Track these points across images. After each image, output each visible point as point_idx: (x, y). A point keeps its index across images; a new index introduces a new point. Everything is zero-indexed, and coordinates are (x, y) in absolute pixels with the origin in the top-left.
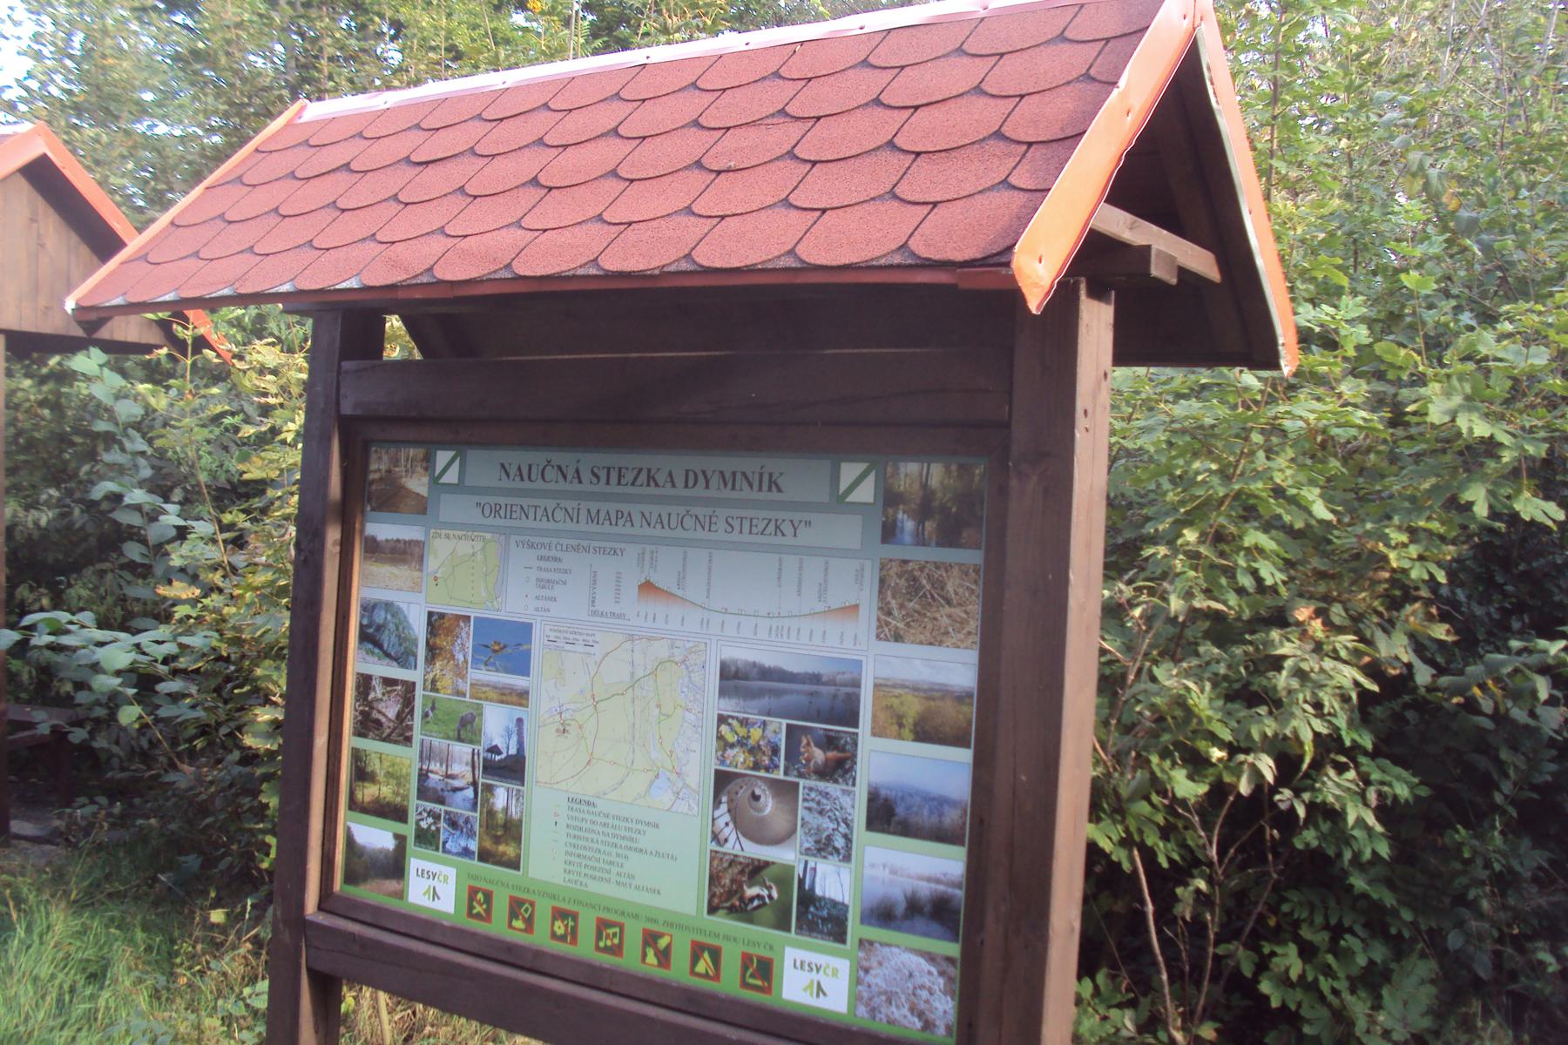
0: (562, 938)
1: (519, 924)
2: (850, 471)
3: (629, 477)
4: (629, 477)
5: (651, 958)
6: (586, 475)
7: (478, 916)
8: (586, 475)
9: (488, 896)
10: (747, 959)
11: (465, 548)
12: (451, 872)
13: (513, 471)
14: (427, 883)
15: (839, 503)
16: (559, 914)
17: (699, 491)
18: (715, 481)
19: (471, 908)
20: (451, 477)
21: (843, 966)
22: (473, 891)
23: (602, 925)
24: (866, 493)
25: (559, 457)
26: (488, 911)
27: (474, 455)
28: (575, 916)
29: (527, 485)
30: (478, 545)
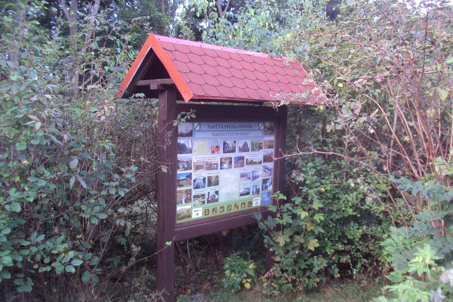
0: (222, 212)
1: (214, 213)
2: (261, 124)
3: (231, 127)
4: (231, 127)
5: (236, 208)
6: (224, 127)
7: (207, 215)
8: (224, 127)
9: (208, 210)
10: (249, 202)
11: (201, 143)
12: (201, 209)
13: (210, 127)
14: (196, 213)
15: (259, 129)
16: (221, 208)
17: (241, 129)
18: (244, 127)
19: (205, 213)
20: (198, 128)
21: (260, 198)
22: (205, 210)
23: (228, 206)
24: (262, 128)
25: (219, 124)
26: (209, 213)
27: (203, 124)
28: (224, 207)
29: (213, 129)
30: (204, 142)
